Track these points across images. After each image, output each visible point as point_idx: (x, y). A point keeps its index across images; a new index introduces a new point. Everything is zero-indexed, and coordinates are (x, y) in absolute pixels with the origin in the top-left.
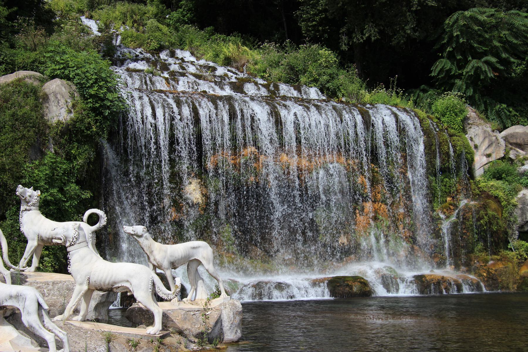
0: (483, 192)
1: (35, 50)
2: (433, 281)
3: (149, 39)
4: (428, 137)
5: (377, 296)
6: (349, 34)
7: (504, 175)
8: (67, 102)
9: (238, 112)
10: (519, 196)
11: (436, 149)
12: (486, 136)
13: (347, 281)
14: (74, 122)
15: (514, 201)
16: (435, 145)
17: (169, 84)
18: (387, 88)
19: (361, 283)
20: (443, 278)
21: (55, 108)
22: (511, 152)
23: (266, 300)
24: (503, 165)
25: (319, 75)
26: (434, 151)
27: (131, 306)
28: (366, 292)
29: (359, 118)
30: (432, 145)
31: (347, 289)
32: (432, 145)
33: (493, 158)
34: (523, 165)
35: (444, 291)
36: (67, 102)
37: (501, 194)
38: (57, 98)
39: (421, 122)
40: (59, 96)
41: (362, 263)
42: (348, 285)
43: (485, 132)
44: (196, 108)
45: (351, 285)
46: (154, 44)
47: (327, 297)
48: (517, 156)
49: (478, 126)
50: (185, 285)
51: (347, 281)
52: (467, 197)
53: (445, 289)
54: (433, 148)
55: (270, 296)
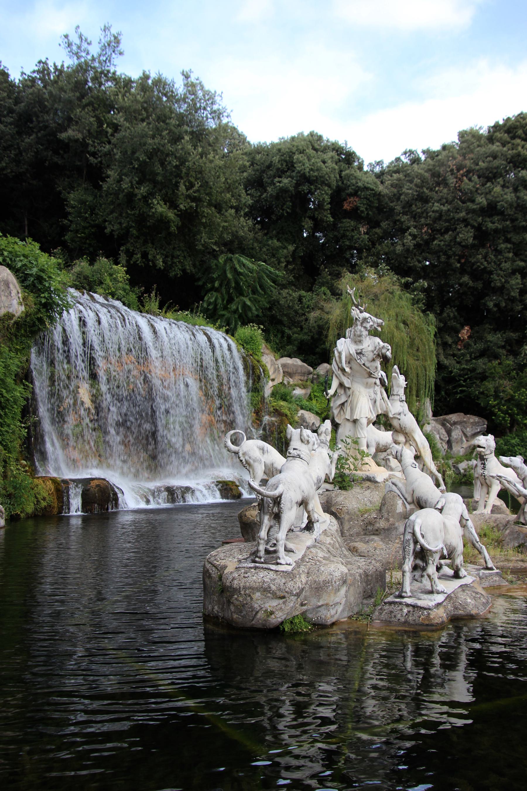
0: (276, 410)
7: (288, 397)
8: (18, 293)
10: (299, 415)
12: (273, 364)
14: (27, 315)
15: (296, 418)
18: (192, 312)
21: (3, 298)
22: (286, 379)
24: (283, 390)
33: (275, 383)
34: (294, 389)
36: (18, 293)
37: (288, 413)
38: (9, 287)
40: (11, 286)
43: (272, 360)
48: (289, 383)
49: (267, 354)
52: (269, 414)
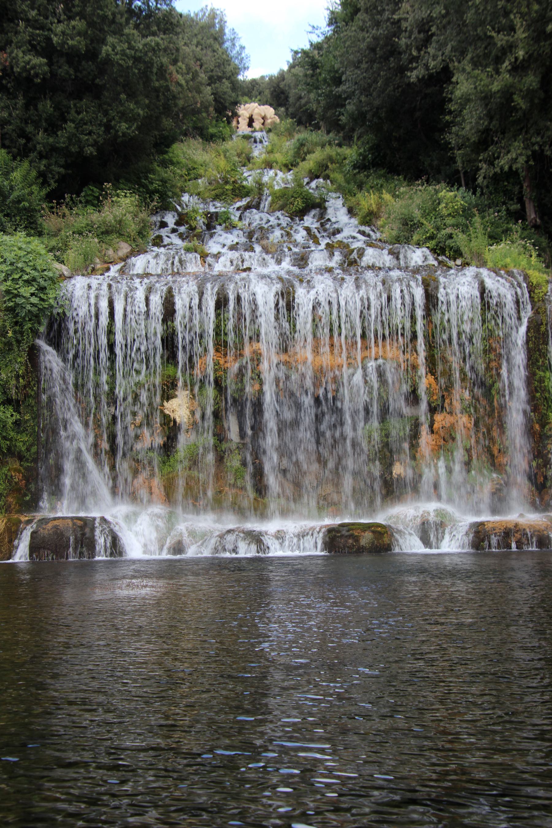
1: (55, 235)
2: (494, 530)
3: (292, 197)
4: (537, 311)
5: (405, 551)
6: (491, 163)
9: (232, 297)
11: (547, 331)
13: (353, 530)
16: (546, 324)
17: (205, 262)
19: (373, 532)
20: (516, 525)
23: (227, 555)
25: (438, 229)
26: (543, 334)
27: (9, 559)
28: (384, 545)
29: (419, 293)
30: (542, 324)
31: (350, 541)
32: (542, 324)
35: (514, 545)
39: (531, 289)
41: (402, 503)
42: (351, 536)
44: (173, 296)
45: (356, 536)
46: (299, 204)
47: (319, 553)
50: (119, 534)
51: (353, 530)
53: (516, 542)
54: (543, 329)
55: (235, 550)
